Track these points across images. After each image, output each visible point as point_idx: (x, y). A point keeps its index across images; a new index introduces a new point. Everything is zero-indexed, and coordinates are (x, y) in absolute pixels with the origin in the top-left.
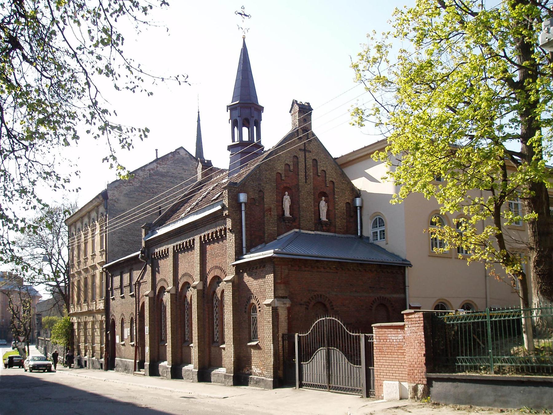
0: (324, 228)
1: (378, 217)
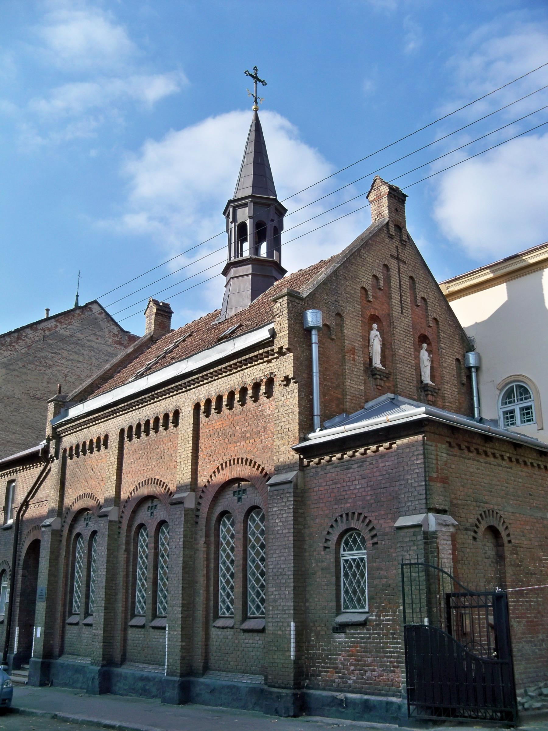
0: (430, 397)
1: (514, 384)
